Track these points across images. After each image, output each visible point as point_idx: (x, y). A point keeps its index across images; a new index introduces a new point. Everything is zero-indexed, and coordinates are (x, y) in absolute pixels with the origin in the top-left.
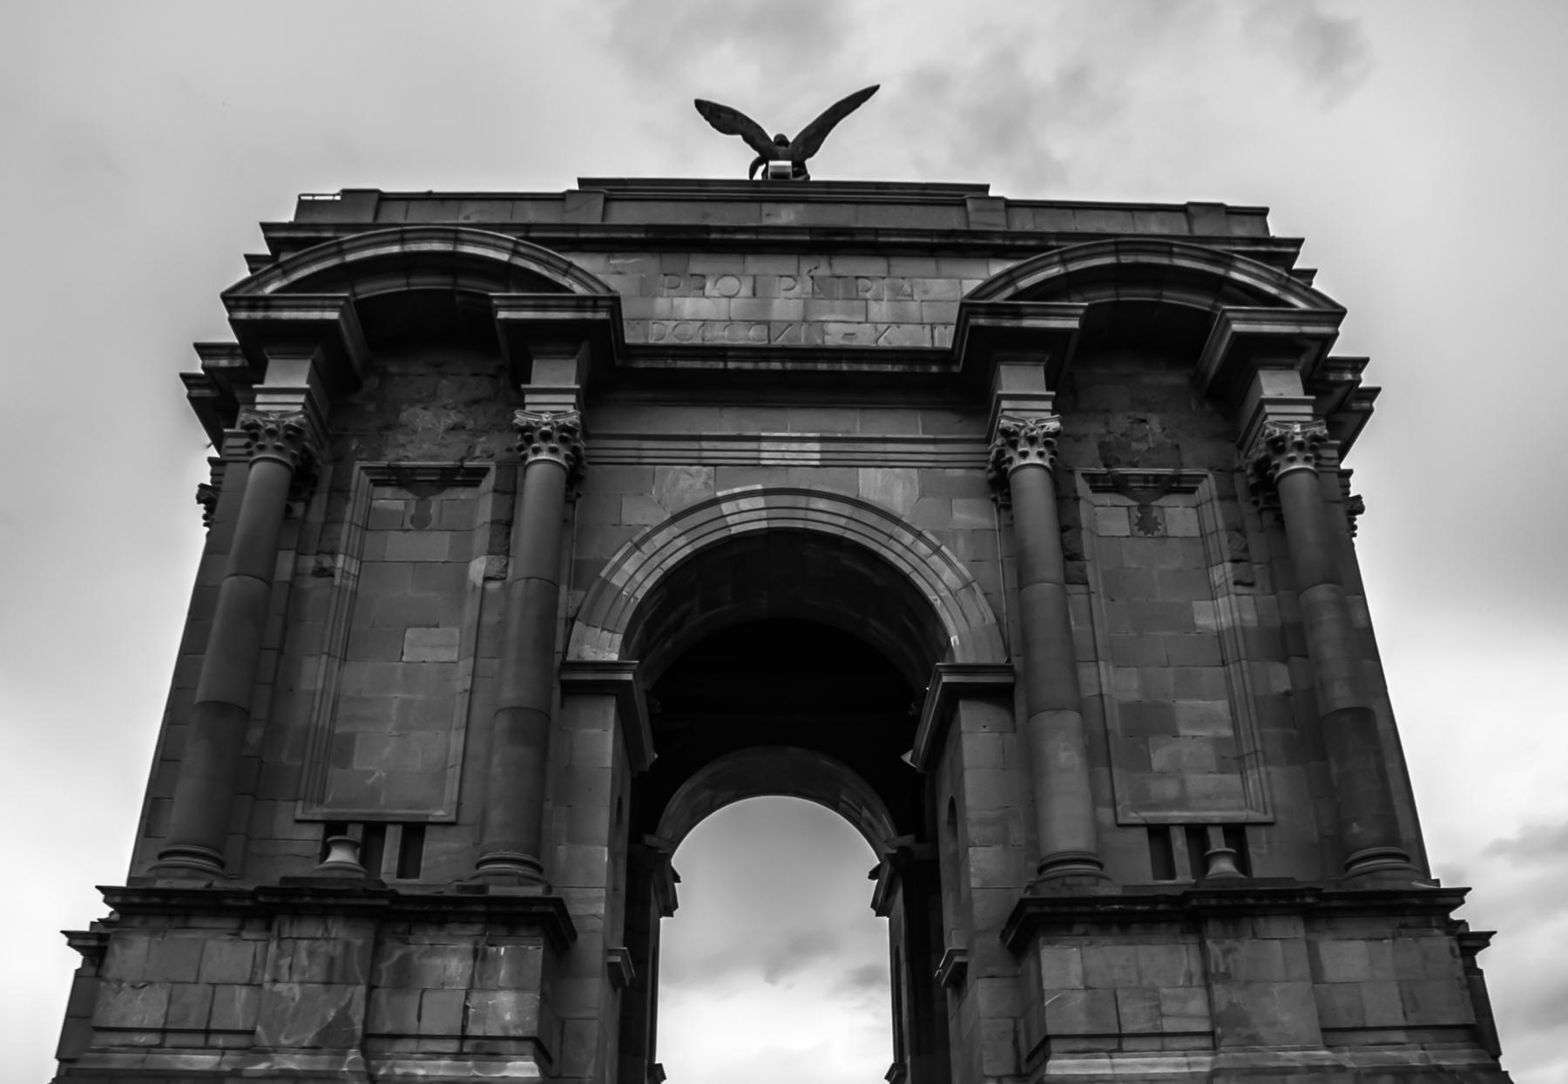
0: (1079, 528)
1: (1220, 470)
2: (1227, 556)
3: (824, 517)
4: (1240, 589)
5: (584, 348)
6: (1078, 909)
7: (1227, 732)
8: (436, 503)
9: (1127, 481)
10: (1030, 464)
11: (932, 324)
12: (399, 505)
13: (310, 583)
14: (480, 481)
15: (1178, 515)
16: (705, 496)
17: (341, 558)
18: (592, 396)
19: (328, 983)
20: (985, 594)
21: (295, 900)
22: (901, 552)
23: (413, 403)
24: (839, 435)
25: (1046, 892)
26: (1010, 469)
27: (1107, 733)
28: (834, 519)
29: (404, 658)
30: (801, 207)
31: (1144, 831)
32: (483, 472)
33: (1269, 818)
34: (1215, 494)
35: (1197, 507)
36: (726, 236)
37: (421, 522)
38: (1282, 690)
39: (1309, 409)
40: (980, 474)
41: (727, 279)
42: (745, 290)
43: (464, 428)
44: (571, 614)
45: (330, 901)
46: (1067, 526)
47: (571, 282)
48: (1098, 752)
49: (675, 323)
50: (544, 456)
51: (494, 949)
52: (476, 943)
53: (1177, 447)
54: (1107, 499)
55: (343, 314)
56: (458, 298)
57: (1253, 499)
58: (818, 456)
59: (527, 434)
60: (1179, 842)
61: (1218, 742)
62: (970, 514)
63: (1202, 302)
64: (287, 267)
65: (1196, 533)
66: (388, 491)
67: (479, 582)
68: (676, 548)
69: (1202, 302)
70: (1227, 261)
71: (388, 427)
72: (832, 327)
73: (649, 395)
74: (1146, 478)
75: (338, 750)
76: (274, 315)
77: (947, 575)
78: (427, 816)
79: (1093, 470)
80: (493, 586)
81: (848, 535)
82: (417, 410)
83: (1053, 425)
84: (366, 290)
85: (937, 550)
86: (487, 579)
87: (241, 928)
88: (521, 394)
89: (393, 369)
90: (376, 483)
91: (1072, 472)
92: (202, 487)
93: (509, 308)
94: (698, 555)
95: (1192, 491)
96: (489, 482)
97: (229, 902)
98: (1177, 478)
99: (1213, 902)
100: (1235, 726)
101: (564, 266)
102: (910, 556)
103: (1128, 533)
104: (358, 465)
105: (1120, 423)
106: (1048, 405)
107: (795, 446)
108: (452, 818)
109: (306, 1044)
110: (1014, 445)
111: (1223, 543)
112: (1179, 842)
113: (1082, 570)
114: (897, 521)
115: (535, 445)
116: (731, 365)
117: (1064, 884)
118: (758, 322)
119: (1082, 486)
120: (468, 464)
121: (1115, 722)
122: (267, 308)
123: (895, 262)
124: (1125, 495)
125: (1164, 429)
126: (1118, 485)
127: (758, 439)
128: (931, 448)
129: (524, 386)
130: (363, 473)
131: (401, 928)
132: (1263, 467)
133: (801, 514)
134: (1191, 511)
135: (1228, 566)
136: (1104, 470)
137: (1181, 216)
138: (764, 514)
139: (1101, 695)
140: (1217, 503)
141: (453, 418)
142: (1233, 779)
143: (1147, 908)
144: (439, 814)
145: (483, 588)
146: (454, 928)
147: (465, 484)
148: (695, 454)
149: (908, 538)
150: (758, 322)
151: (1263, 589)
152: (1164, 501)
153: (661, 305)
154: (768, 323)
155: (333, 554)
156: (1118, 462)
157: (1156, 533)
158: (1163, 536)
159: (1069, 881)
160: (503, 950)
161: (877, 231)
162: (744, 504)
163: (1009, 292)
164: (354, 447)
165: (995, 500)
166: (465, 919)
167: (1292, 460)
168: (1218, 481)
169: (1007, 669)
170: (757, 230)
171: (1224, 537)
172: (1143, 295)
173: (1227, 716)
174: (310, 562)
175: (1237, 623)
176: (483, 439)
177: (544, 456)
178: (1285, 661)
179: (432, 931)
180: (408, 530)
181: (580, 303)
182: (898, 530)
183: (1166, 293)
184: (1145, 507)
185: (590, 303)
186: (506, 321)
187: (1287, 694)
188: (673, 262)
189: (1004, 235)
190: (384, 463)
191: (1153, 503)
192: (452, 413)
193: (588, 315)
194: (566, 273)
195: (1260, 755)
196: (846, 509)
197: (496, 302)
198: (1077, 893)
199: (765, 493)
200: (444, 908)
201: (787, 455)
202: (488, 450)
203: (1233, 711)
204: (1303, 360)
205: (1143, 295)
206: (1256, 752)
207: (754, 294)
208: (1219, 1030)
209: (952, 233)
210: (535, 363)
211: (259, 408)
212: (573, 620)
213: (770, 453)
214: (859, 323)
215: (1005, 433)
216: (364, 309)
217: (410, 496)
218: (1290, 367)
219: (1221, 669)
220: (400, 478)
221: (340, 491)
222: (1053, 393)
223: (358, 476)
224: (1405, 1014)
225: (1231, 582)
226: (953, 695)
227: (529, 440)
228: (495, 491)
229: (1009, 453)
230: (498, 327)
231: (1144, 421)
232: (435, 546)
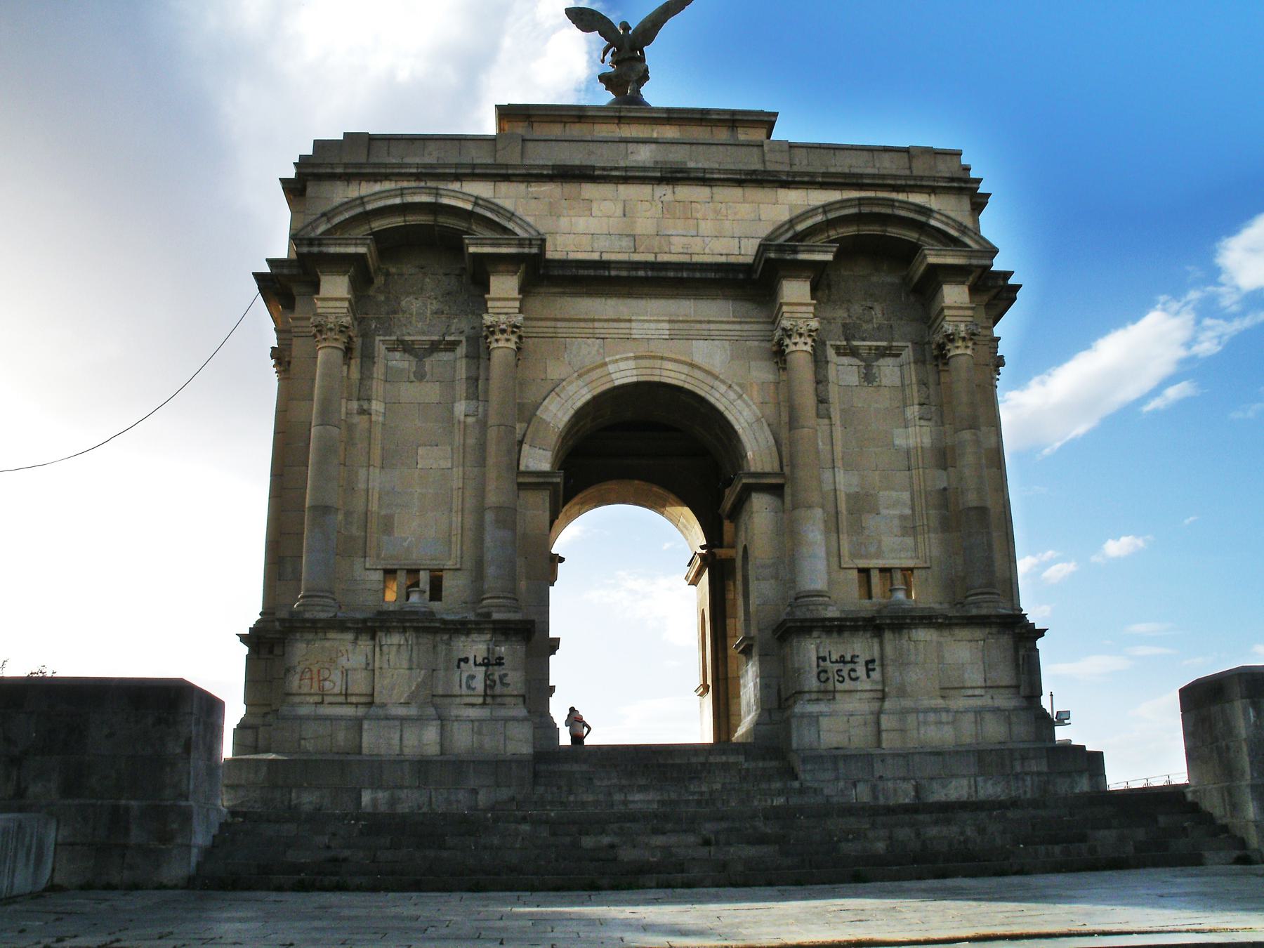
0: (827, 381)
1: (916, 343)
2: (916, 401)
3: (672, 375)
4: (923, 422)
5: (523, 267)
6: (815, 624)
7: (908, 511)
8: (429, 362)
9: (858, 350)
10: (800, 348)
11: (739, 238)
12: (406, 364)
13: (356, 419)
15: (888, 371)
16: (599, 361)
17: (374, 402)
19: (410, 669)
20: (769, 425)
21: (388, 624)
22: (720, 398)
23: (408, 294)
24: (681, 318)
25: (799, 614)
26: (787, 352)
27: (837, 513)
28: (678, 375)
29: (419, 466)
30: (653, 146)
31: (856, 571)
32: (458, 343)
33: (928, 565)
34: (912, 360)
36: (605, 173)
37: (420, 376)
38: (942, 487)
39: (970, 313)
40: (768, 345)
41: (607, 203)
42: (619, 212)
43: (442, 313)
44: (520, 439)
45: (408, 624)
46: (820, 381)
47: (513, 225)
48: (833, 525)
50: (501, 344)
51: (498, 648)
52: (488, 645)
53: (891, 326)
54: (845, 360)
55: (369, 248)
56: (437, 229)
57: (935, 363)
58: (667, 332)
59: (491, 329)
61: (902, 517)
62: (762, 373)
63: (912, 236)
64: (330, 215)
65: (899, 384)
66: (398, 355)
67: (462, 418)
68: (579, 394)
69: (912, 236)
70: (928, 213)
71: (395, 312)
72: (674, 240)
73: (560, 290)
74: (870, 348)
75: (388, 525)
76: (325, 249)
77: (746, 412)
78: (444, 565)
79: (838, 343)
80: (470, 420)
81: (686, 386)
82: (411, 298)
83: (814, 324)
84: (377, 225)
85: (740, 397)
86: (466, 416)
87: (356, 639)
88: (486, 302)
89: (393, 270)
90: (389, 350)
92: (273, 348)
93: (476, 245)
94: (595, 399)
95: (898, 356)
96: (461, 350)
97: (350, 625)
98: (890, 348)
99: (888, 621)
100: (913, 509)
101: (509, 215)
102: (724, 400)
103: (857, 384)
104: (378, 338)
105: (857, 309)
106: (811, 309)
107: (653, 326)
108: (458, 566)
109: (402, 701)
110: (790, 337)
111: (914, 393)
112: (875, 578)
113: (828, 410)
114: (716, 378)
115: (496, 337)
116: (613, 273)
117: (808, 610)
118: (628, 235)
119: (831, 353)
120: (448, 338)
121: (843, 507)
122: (320, 245)
123: (715, 190)
124: (857, 358)
125: (883, 314)
126: (854, 352)
127: (630, 321)
128: (737, 327)
129: (487, 296)
130: (381, 343)
131: (446, 637)
132: (941, 347)
133: (658, 372)
134: (897, 369)
135: (917, 407)
136: (845, 343)
137: (905, 155)
138: (635, 372)
139: (835, 490)
140: (912, 366)
141: (435, 306)
142: (909, 541)
143: (852, 624)
144: (449, 564)
145: (465, 422)
146: (474, 636)
147: (446, 350)
148: (591, 331)
149: (723, 388)
150: (628, 235)
151: (936, 422)
152: (882, 362)
153: (564, 222)
154: (634, 236)
155: (369, 400)
156: (854, 338)
157: (875, 384)
158: (879, 386)
159: (811, 607)
161: (704, 170)
162: (623, 365)
163: (789, 235)
164: (373, 326)
165: (777, 363)
166: (480, 631)
167: (957, 347)
168: (914, 350)
169: (781, 474)
170: (626, 169)
171: (915, 388)
172: (875, 230)
173: (909, 503)
174: (355, 405)
175: (919, 445)
176: (456, 320)
177: (501, 344)
178: (945, 469)
179: (463, 638)
180: (411, 382)
181: (521, 242)
182: (717, 383)
183: (889, 229)
184: (868, 367)
185: (527, 242)
186: (475, 255)
187: (945, 489)
188: (570, 188)
189: (788, 173)
190: (394, 338)
191: (874, 364)
192: (434, 302)
193: (526, 250)
194: (510, 219)
195: (926, 528)
196: (685, 369)
197: (467, 241)
198: (815, 615)
199: (636, 358)
200: (470, 626)
201: (649, 332)
202: (460, 327)
203: (912, 499)
204: (971, 279)
205: (875, 230)
206: (923, 525)
207: (624, 215)
208: (887, 689)
209: (754, 172)
210: (492, 279)
211: (319, 311)
212: (521, 443)
213: (637, 330)
215: (784, 329)
216: (378, 236)
217: (411, 358)
218: (963, 283)
219: (907, 473)
220: (405, 347)
221: (368, 357)
222: (815, 302)
223: (380, 349)
224: (985, 681)
225: (917, 418)
226: (748, 490)
227: (493, 333)
228: (467, 357)
229: (787, 341)
230: (467, 256)
231: (871, 308)
232: (430, 392)
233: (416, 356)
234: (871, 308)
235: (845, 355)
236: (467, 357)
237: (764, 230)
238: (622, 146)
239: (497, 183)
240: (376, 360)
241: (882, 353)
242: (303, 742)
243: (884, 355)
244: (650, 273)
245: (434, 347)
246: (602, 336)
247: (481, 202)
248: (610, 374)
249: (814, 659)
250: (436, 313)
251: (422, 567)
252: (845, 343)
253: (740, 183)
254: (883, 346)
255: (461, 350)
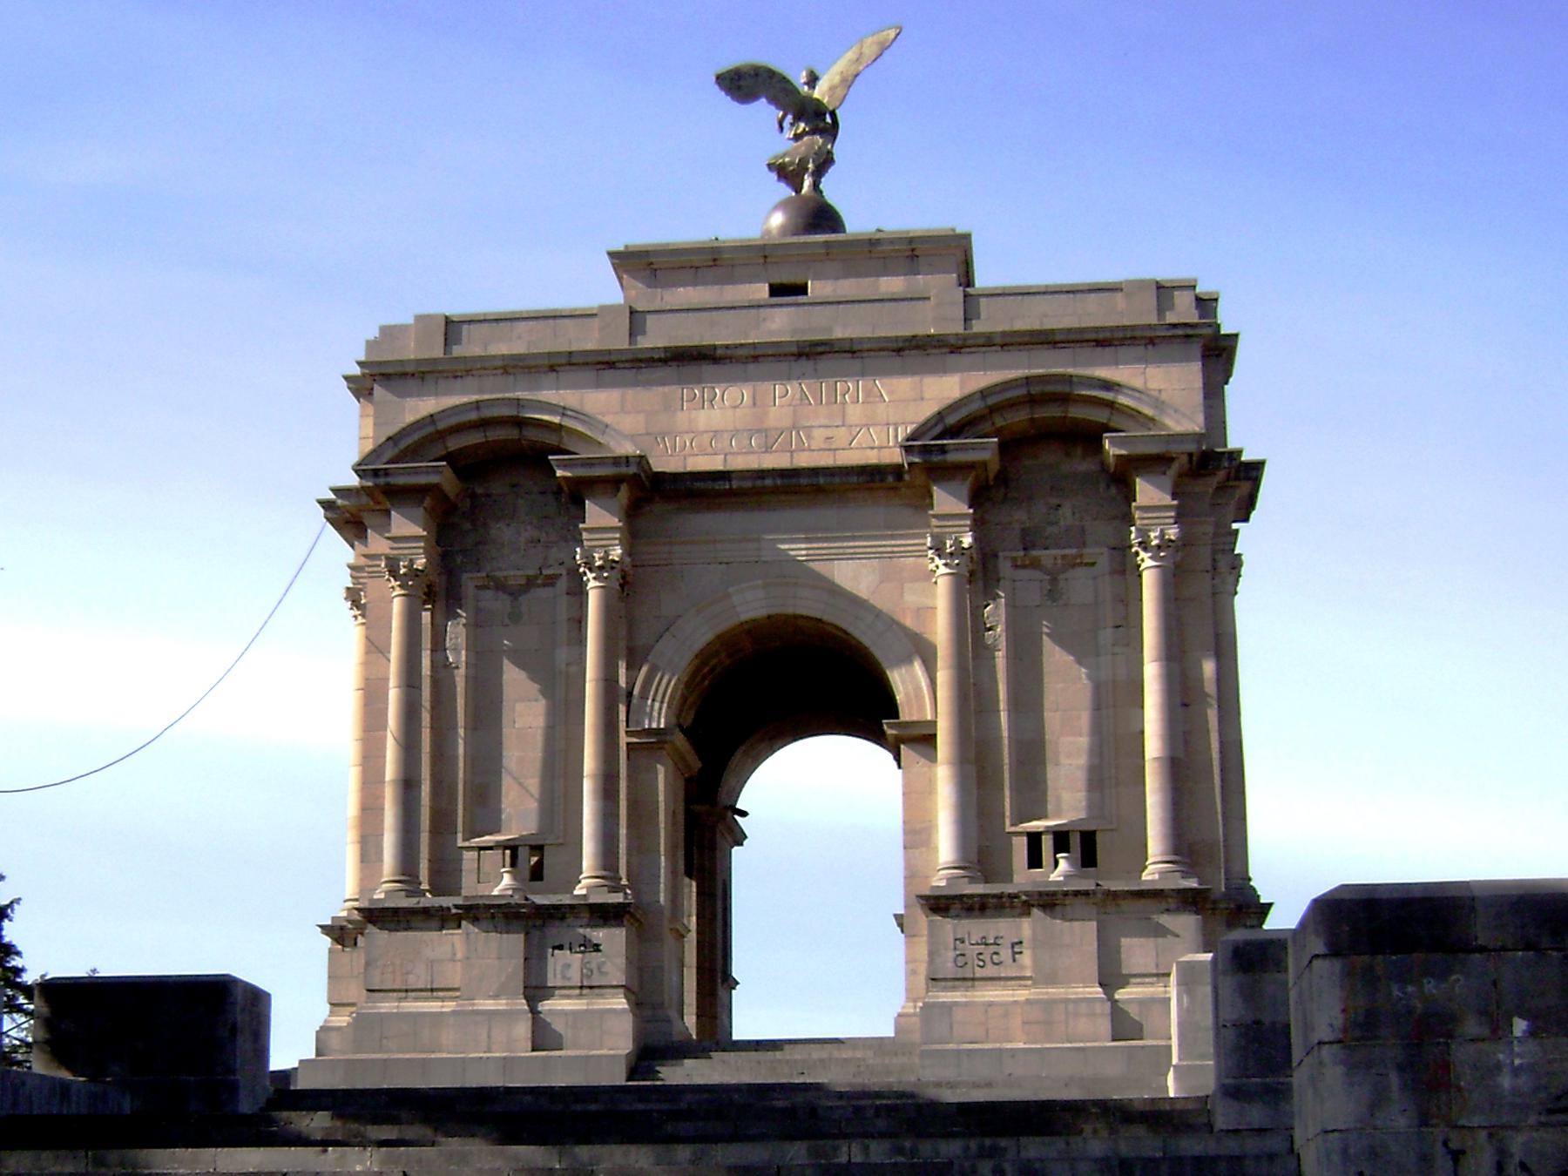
4: (1117, 649)
14: (555, 583)
18: (632, 513)
29: (517, 726)
35: (1095, 578)
37: (515, 617)
49: (693, 435)
60: (1047, 844)
63: (1100, 416)
66: (489, 593)
67: (563, 666)
70: (1116, 388)
79: (1014, 554)
82: (501, 525)
84: (454, 444)
86: (567, 665)
89: (479, 491)
91: (996, 556)
92: (348, 589)
95: (1093, 564)
96: (562, 584)
108: (561, 841)
109: (491, 994)
116: (735, 485)
125: (1074, 513)
126: (1035, 564)
129: (581, 526)
131: (539, 922)
147: (544, 585)
152: (1070, 574)
153: (681, 418)
156: (1034, 546)
160: (601, 934)
179: (557, 923)
180: (507, 625)
192: (529, 527)
207: (754, 404)
214: (837, 426)
218: (1164, 473)
224: (1157, 966)
233: (511, 594)
234: (1059, 506)
235: (1024, 567)
236: (568, 594)
237: (927, 410)
238: (753, 311)
239: (600, 372)
240: (463, 601)
241: (1073, 564)
242: (385, 1041)
243: (1074, 566)
244: (779, 482)
245: (530, 583)
246: (725, 560)
247: (569, 413)
248: (734, 607)
249: (952, 940)
250: (532, 542)
251: (522, 843)
252: (1021, 553)
253: (899, 351)
254: (1072, 555)
255: (562, 584)
